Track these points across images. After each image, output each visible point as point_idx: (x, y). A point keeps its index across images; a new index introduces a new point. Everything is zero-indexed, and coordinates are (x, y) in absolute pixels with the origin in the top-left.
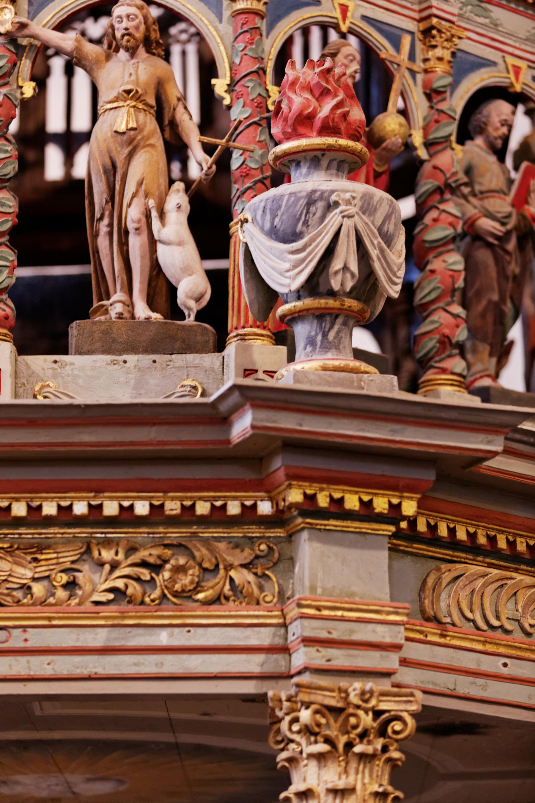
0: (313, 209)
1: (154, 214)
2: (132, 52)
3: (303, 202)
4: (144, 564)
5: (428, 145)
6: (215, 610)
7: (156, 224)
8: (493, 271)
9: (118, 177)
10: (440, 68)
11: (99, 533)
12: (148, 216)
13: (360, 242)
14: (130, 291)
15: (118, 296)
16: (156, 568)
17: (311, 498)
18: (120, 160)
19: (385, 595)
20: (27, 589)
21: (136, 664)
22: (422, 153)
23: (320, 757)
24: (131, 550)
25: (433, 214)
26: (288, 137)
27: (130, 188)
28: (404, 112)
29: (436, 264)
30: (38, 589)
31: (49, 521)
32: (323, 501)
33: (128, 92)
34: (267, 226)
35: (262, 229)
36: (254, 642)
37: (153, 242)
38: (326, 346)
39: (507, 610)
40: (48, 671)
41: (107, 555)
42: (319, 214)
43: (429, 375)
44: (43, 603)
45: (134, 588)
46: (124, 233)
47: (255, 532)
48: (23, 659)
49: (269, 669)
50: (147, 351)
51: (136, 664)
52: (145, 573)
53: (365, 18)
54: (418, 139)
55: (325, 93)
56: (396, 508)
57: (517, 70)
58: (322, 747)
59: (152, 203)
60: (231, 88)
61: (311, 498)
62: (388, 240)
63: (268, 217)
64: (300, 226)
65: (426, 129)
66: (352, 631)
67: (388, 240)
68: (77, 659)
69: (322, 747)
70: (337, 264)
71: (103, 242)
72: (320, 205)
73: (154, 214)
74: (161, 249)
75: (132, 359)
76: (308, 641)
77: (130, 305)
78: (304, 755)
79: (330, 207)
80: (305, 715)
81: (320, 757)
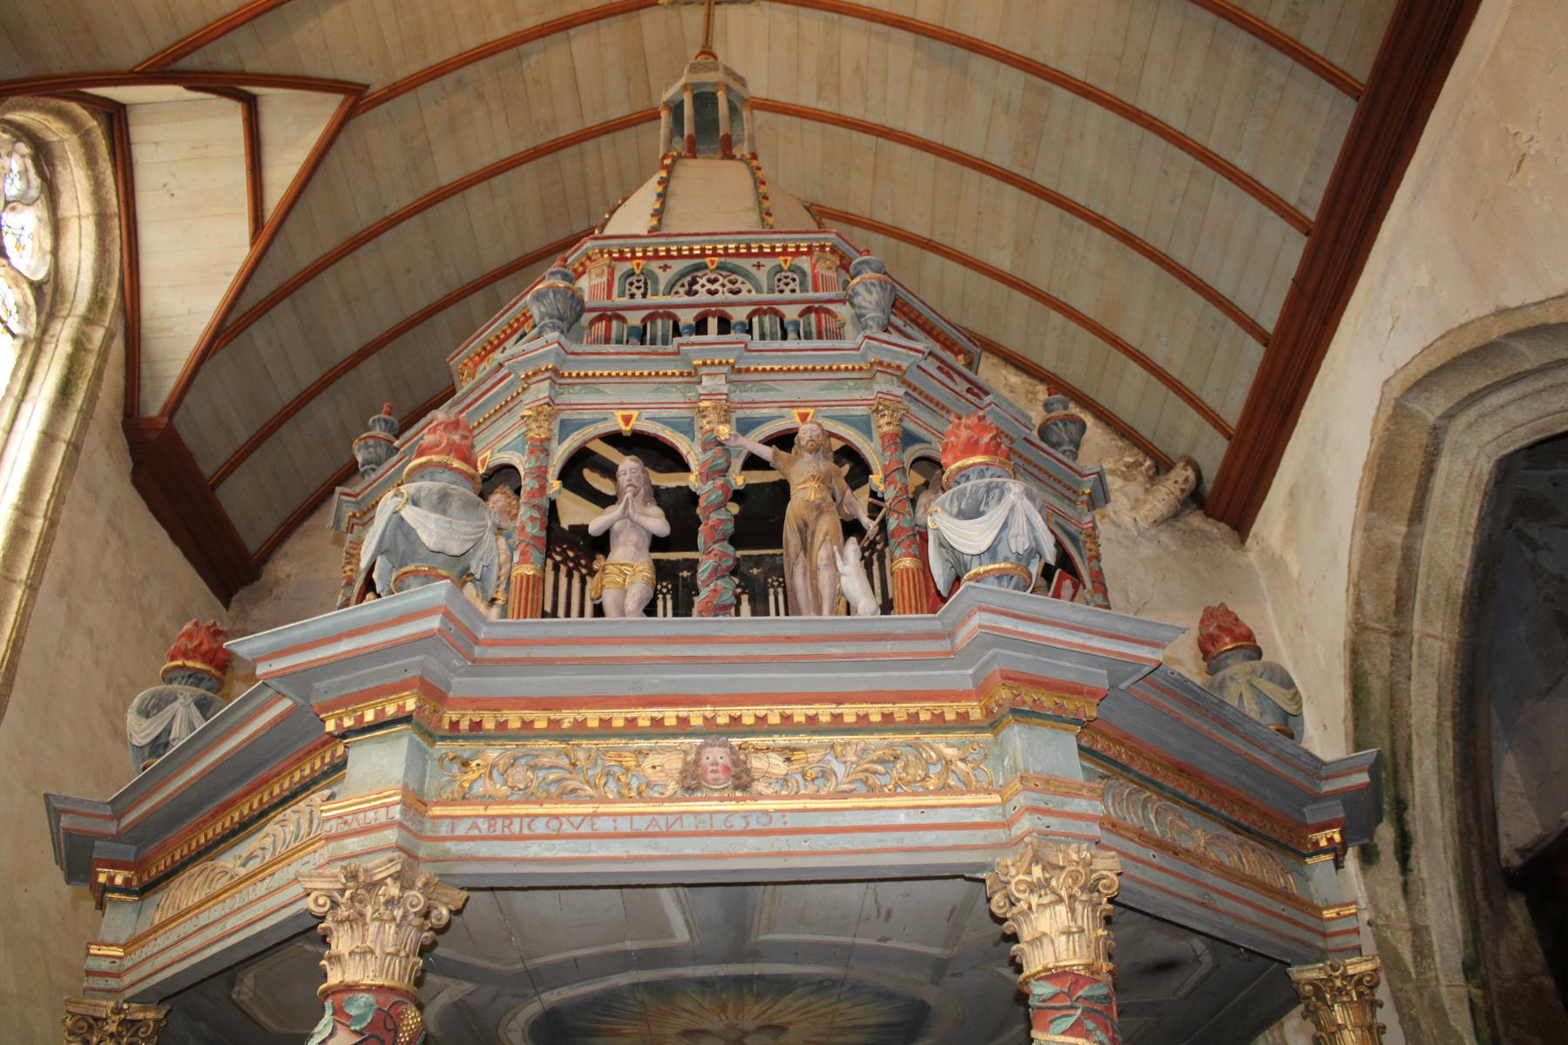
0: (991, 494)
1: (838, 556)
3: (983, 490)
4: (880, 761)
7: (839, 563)
9: (809, 533)
12: (834, 557)
13: (1028, 520)
21: (880, 841)
26: (956, 459)
27: (819, 539)
33: (813, 476)
34: (955, 510)
35: (951, 514)
36: (978, 819)
37: (836, 576)
40: (805, 847)
42: (996, 498)
48: (783, 838)
49: (990, 840)
51: (880, 841)
59: (835, 548)
63: (956, 504)
64: (982, 508)
66: (1063, 804)
68: (829, 837)
70: (1013, 530)
72: (997, 492)
73: (838, 556)
74: (843, 579)
78: (1034, 908)
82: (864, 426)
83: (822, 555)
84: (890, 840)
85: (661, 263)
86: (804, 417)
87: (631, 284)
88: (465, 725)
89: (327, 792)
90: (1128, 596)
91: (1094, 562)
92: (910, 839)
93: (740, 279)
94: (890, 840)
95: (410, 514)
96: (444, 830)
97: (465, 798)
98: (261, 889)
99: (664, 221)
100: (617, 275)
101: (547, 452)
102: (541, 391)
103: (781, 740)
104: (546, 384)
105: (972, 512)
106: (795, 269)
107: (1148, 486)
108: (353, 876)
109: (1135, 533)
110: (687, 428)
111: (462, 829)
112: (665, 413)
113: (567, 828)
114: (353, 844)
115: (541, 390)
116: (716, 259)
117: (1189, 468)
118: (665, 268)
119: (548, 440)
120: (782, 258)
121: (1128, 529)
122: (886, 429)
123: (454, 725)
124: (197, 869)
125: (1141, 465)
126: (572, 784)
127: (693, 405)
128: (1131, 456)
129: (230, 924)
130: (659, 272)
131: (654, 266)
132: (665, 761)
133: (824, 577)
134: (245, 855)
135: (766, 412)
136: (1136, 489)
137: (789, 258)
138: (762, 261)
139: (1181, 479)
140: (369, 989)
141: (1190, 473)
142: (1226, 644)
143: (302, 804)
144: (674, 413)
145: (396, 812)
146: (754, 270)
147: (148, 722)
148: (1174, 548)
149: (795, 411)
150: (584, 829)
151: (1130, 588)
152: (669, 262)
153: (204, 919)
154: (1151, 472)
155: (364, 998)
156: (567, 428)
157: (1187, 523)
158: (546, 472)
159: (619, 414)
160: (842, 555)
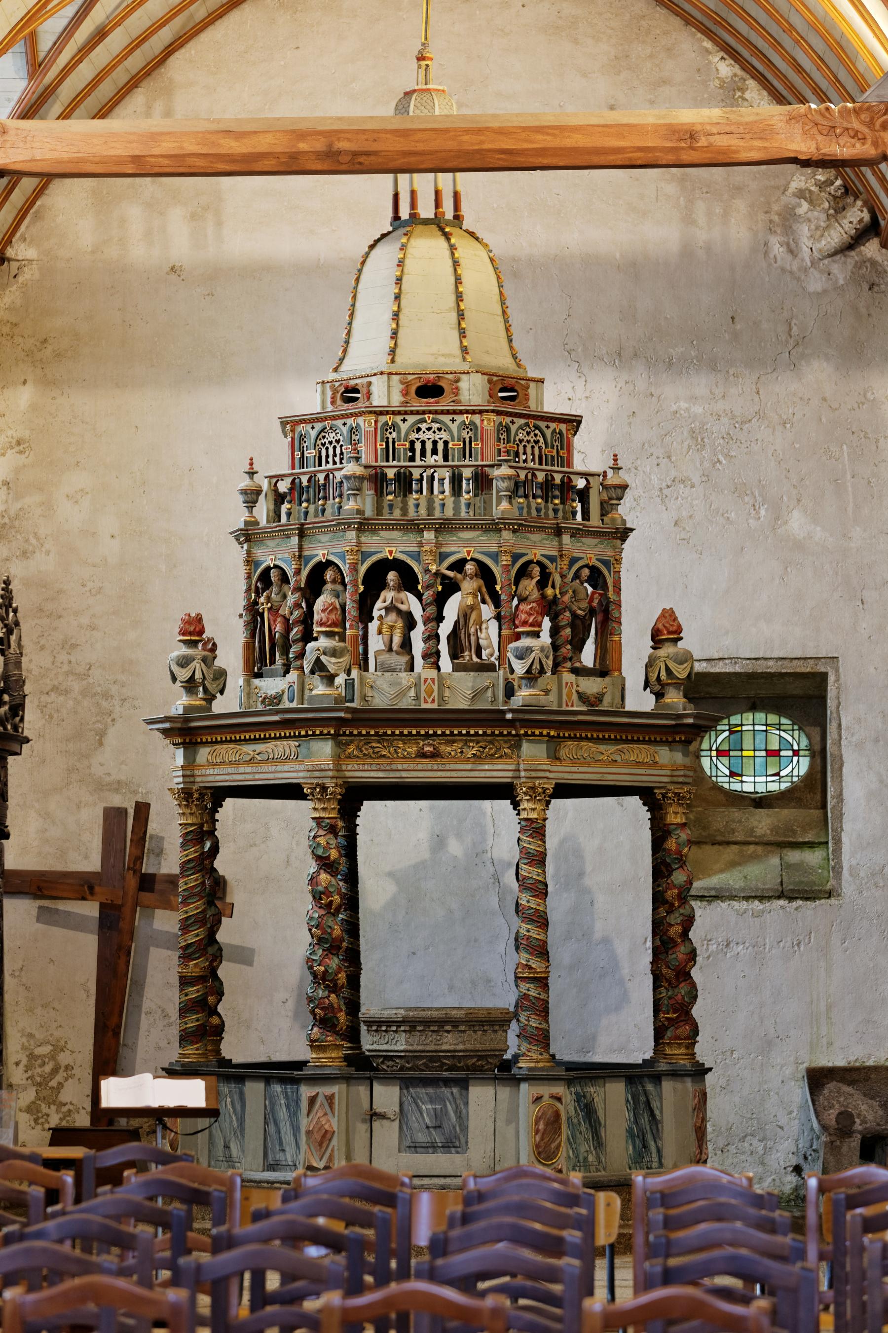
2: (471, 578)
5: (560, 593)
6: (500, 760)
8: (581, 628)
10: (565, 567)
11: (469, 738)
14: (470, 651)
15: (467, 653)
16: (484, 748)
17: (526, 732)
18: (468, 612)
19: (545, 756)
20: (450, 754)
22: (559, 596)
23: (528, 800)
24: (477, 743)
25: (562, 616)
27: (471, 622)
28: (553, 587)
29: (562, 633)
30: (453, 753)
31: (456, 735)
32: (529, 733)
37: (478, 638)
38: (531, 687)
39: (579, 754)
41: (471, 744)
43: (559, 669)
44: (454, 757)
45: (478, 753)
46: (469, 635)
47: (511, 738)
50: (476, 671)
52: (481, 750)
53: (542, 555)
54: (557, 592)
55: (530, 615)
56: (548, 734)
57: (591, 559)
58: (528, 797)
60: (501, 588)
61: (526, 732)
62: (547, 657)
65: (560, 589)
67: (547, 657)
69: (528, 797)
70: (534, 667)
71: (462, 636)
74: (481, 641)
75: (472, 673)
76: (525, 770)
77: (471, 656)
79: (532, 651)
80: (524, 789)
81: (528, 800)
82: (495, 557)
83: (472, 630)
84: (482, 774)
85: (402, 417)
86: (469, 552)
87: (387, 430)
88: (347, 732)
89: (297, 744)
90: (790, 329)
91: (617, 574)
92: (488, 774)
93: (444, 428)
94: (482, 774)
95: (323, 658)
96: (344, 768)
97: (349, 757)
98: (271, 769)
99: (400, 322)
100: (379, 425)
101: (357, 571)
102: (352, 535)
103: (449, 738)
104: (354, 533)
105: (520, 657)
106: (472, 423)
107: (832, 212)
108: (318, 785)
109: (809, 264)
110: (417, 557)
111: (349, 767)
112: (407, 549)
113: (382, 768)
114: (317, 774)
115: (352, 535)
116: (431, 416)
117: (865, 210)
118: (404, 420)
119: (357, 564)
120: (465, 415)
121: (803, 260)
122: (504, 563)
123: (344, 733)
124: (232, 746)
125: (832, 183)
126: (383, 753)
127: (421, 544)
128: (823, 174)
129: (257, 777)
130: (401, 423)
131: (398, 419)
132: (412, 750)
133: (473, 638)
134: (258, 752)
135: (453, 549)
136: (819, 216)
137: (470, 416)
138: (456, 417)
139: (855, 221)
140: (328, 818)
141: (866, 216)
142: (664, 635)
143: (285, 743)
144: (412, 549)
145: (331, 766)
146: (450, 423)
147: (184, 670)
148: (841, 282)
149: (465, 549)
150: (388, 768)
151: (794, 321)
152: (407, 417)
153: (242, 770)
154: (839, 193)
155: (328, 821)
156: (365, 556)
157: (861, 252)
158: (357, 582)
159: (387, 549)
160: (481, 629)
